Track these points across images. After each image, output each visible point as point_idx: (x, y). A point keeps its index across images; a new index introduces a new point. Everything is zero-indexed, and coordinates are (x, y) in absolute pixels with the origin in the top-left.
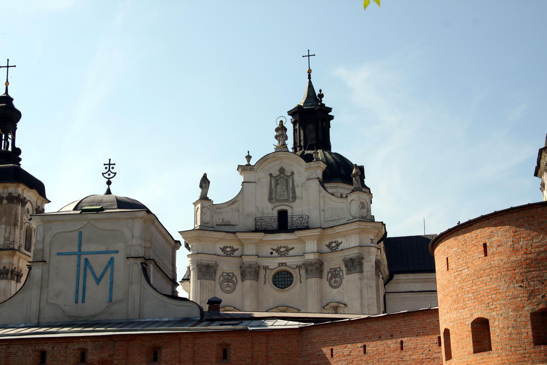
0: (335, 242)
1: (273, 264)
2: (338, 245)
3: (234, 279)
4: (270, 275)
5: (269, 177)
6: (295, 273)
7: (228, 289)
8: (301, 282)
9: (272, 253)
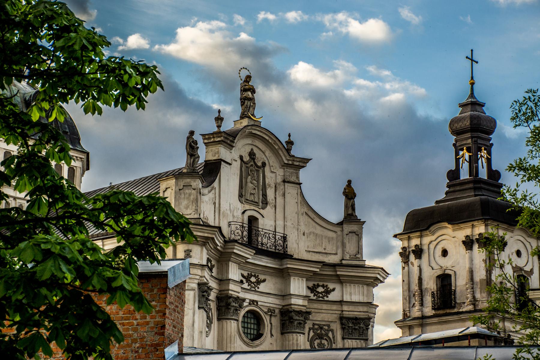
0: (323, 286)
2: (328, 292)
5: (239, 161)
6: (266, 319)
8: (272, 335)
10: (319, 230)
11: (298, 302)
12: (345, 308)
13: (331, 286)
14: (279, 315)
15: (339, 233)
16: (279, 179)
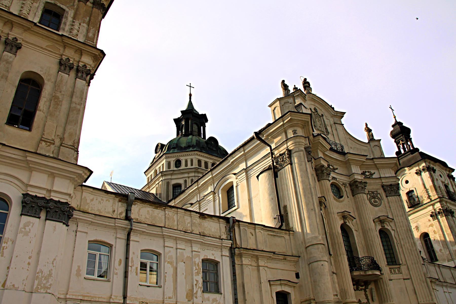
0: (368, 172)
2: (372, 174)
6: (343, 188)
8: (348, 197)
10: (358, 146)
11: (359, 178)
12: (383, 181)
13: (372, 172)
14: (349, 187)
15: (369, 147)
16: (332, 123)
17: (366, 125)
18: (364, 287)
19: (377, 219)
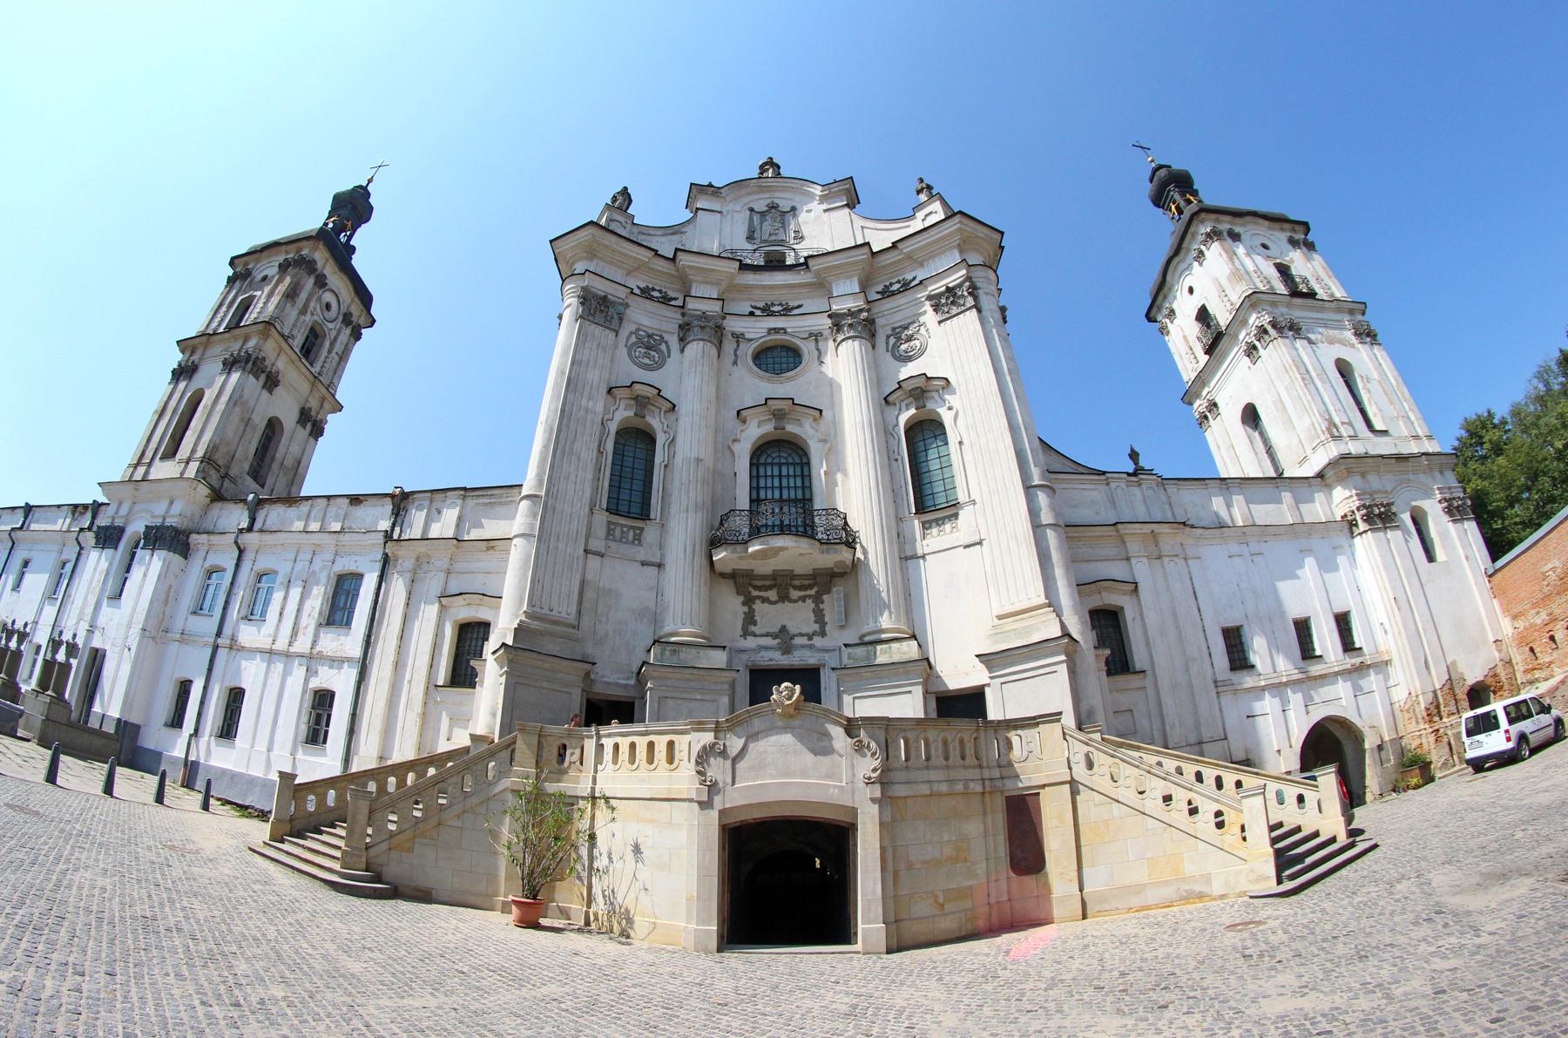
1: (757, 329)
3: (663, 347)
4: (748, 350)
6: (807, 348)
7: (646, 361)
9: (752, 314)
13: (909, 277)
17: (921, 180)
18: (812, 592)
19: (899, 393)
